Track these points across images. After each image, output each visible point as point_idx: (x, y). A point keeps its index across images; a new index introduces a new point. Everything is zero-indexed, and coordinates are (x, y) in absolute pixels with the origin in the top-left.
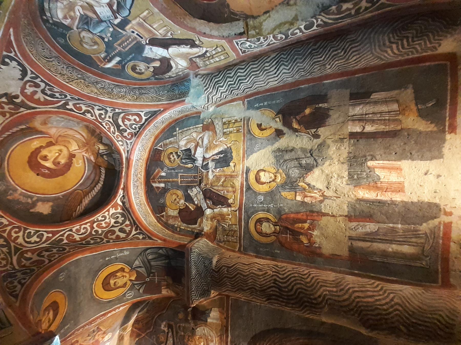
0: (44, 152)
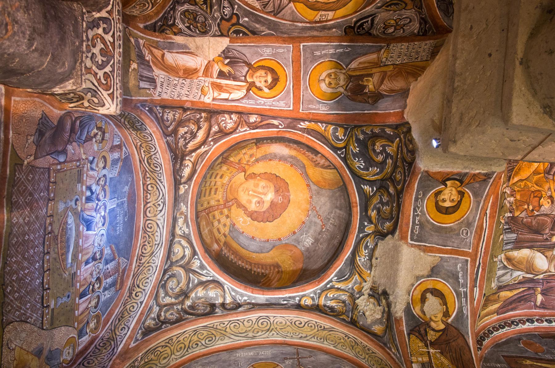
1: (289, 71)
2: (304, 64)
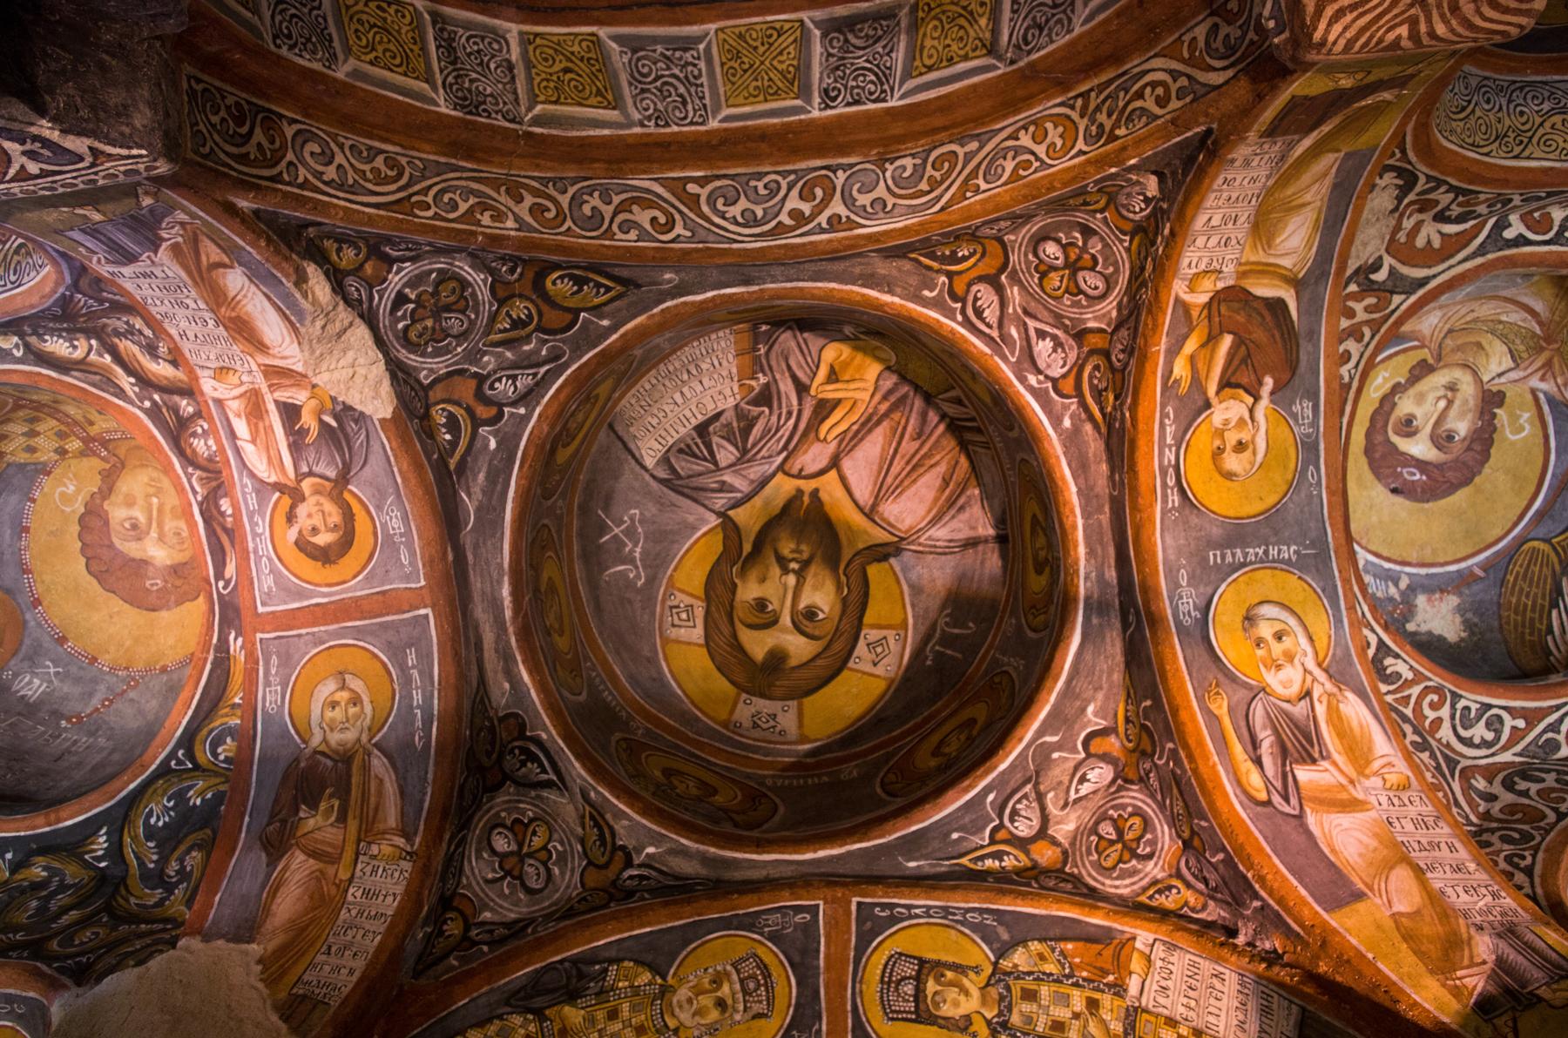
0: (1405, 406)
1: (356, 588)
2: (380, 624)
